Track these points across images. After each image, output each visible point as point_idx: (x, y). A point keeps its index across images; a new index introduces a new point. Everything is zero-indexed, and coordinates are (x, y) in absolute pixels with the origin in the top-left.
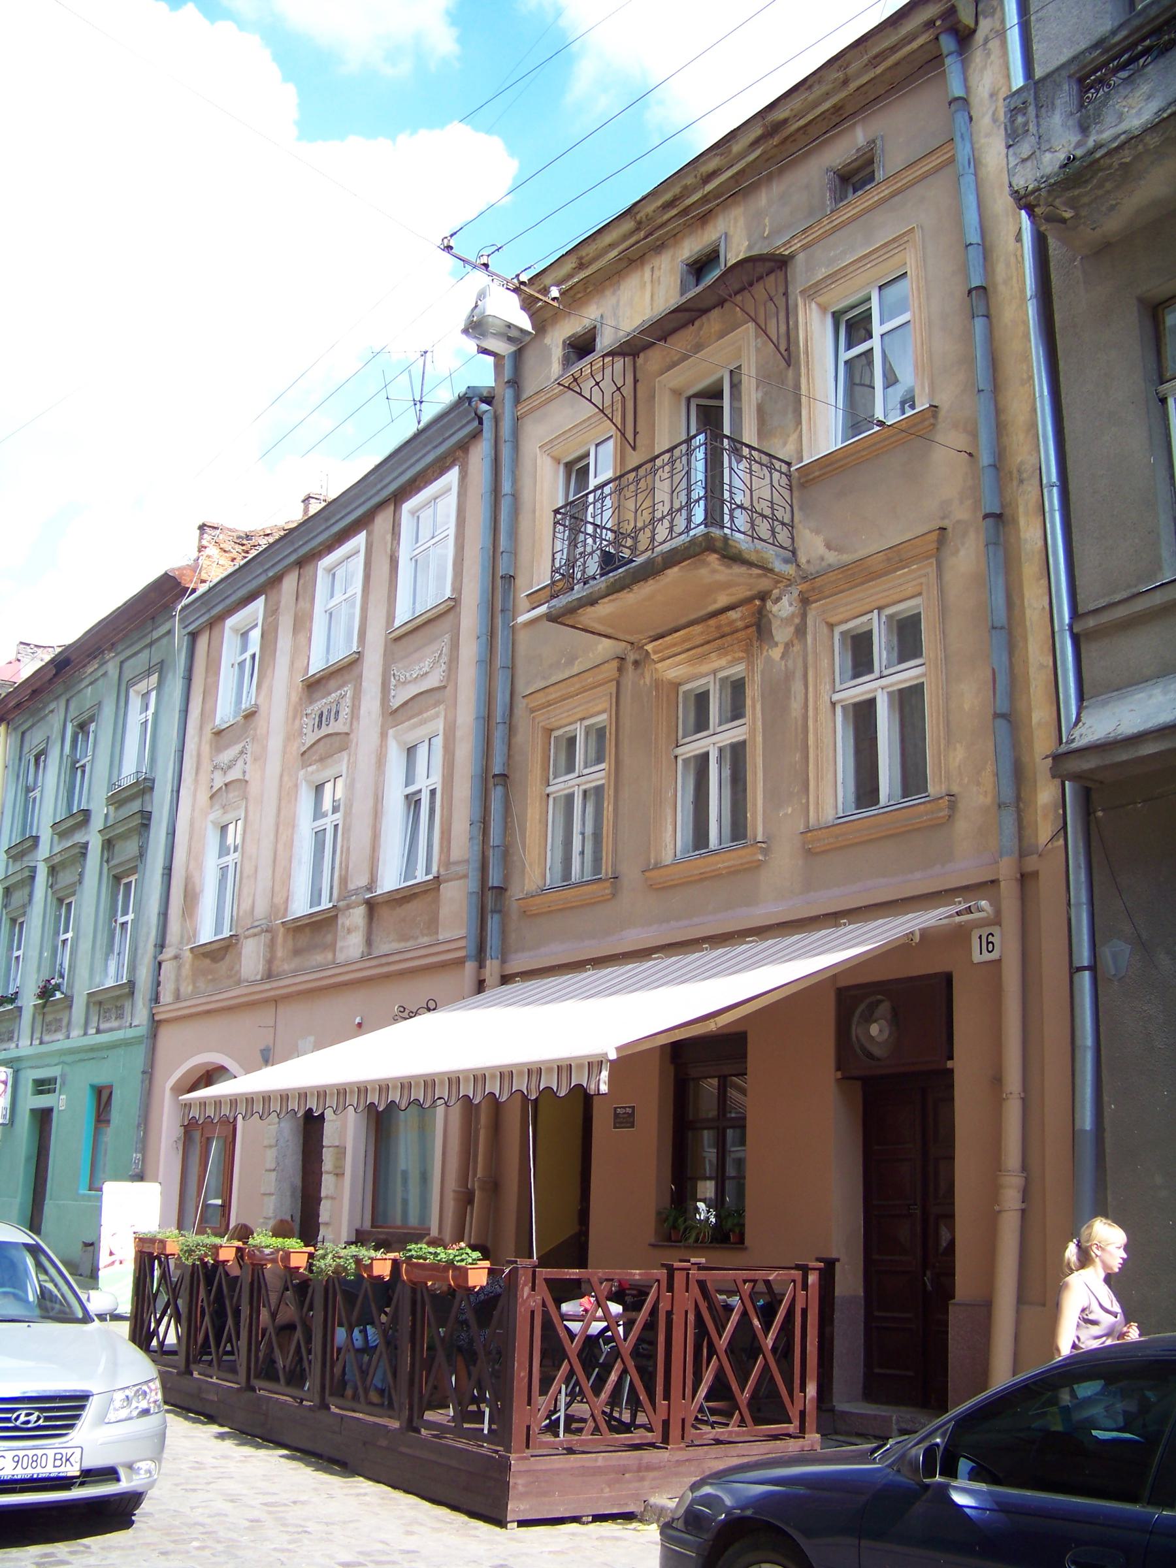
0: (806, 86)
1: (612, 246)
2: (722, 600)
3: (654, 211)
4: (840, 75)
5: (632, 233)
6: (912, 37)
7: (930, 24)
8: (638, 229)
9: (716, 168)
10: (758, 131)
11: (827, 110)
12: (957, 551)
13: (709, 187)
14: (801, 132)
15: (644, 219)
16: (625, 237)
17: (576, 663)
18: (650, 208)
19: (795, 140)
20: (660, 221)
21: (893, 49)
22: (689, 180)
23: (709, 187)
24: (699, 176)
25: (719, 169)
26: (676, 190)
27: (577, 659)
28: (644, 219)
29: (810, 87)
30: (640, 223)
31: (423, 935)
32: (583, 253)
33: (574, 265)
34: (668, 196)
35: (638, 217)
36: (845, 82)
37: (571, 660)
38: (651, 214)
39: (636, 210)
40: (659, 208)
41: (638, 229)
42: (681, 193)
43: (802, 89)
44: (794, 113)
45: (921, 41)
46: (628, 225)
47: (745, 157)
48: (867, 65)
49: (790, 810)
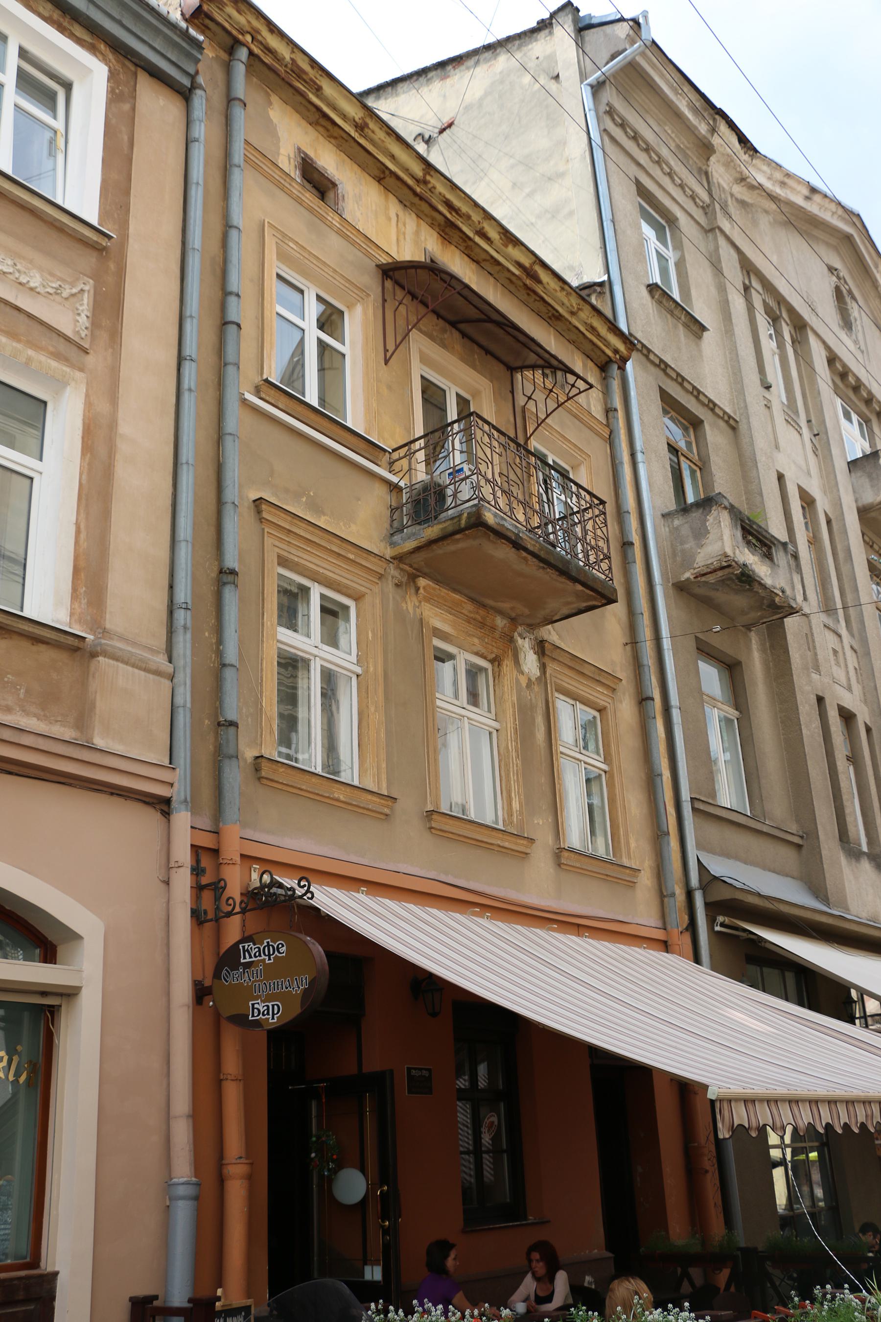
0: (562, 286)
1: (393, 157)
2: (506, 606)
3: (440, 194)
4: (575, 310)
5: (413, 176)
6: (608, 344)
7: (616, 351)
8: (418, 181)
9: (492, 239)
10: (526, 261)
11: (557, 311)
12: (621, 702)
13: (477, 239)
14: (538, 299)
15: (430, 186)
16: (406, 170)
17: (323, 518)
18: (441, 188)
19: (528, 294)
20: (435, 202)
21: (598, 336)
22: (476, 217)
23: (477, 239)
24: (481, 225)
25: (492, 242)
26: (465, 208)
27: (324, 514)
28: (430, 186)
29: (562, 289)
30: (425, 182)
31: (27, 713)
32: (372, 125)
33: (357, 119)
34: (457, 203)
35: (428, 178)
36: (573, 313)
37: (319, 511)
38: (437, 191)
39: (432, 173)
40: (444, 197)
41: (418, 181)
42: (464, 214)
43: (561, 284)
44: (547, 286)
45: (609, 353)
46: (417, 169)
47: (508, 261)
48: (586, 323)
49: (541, 823)
